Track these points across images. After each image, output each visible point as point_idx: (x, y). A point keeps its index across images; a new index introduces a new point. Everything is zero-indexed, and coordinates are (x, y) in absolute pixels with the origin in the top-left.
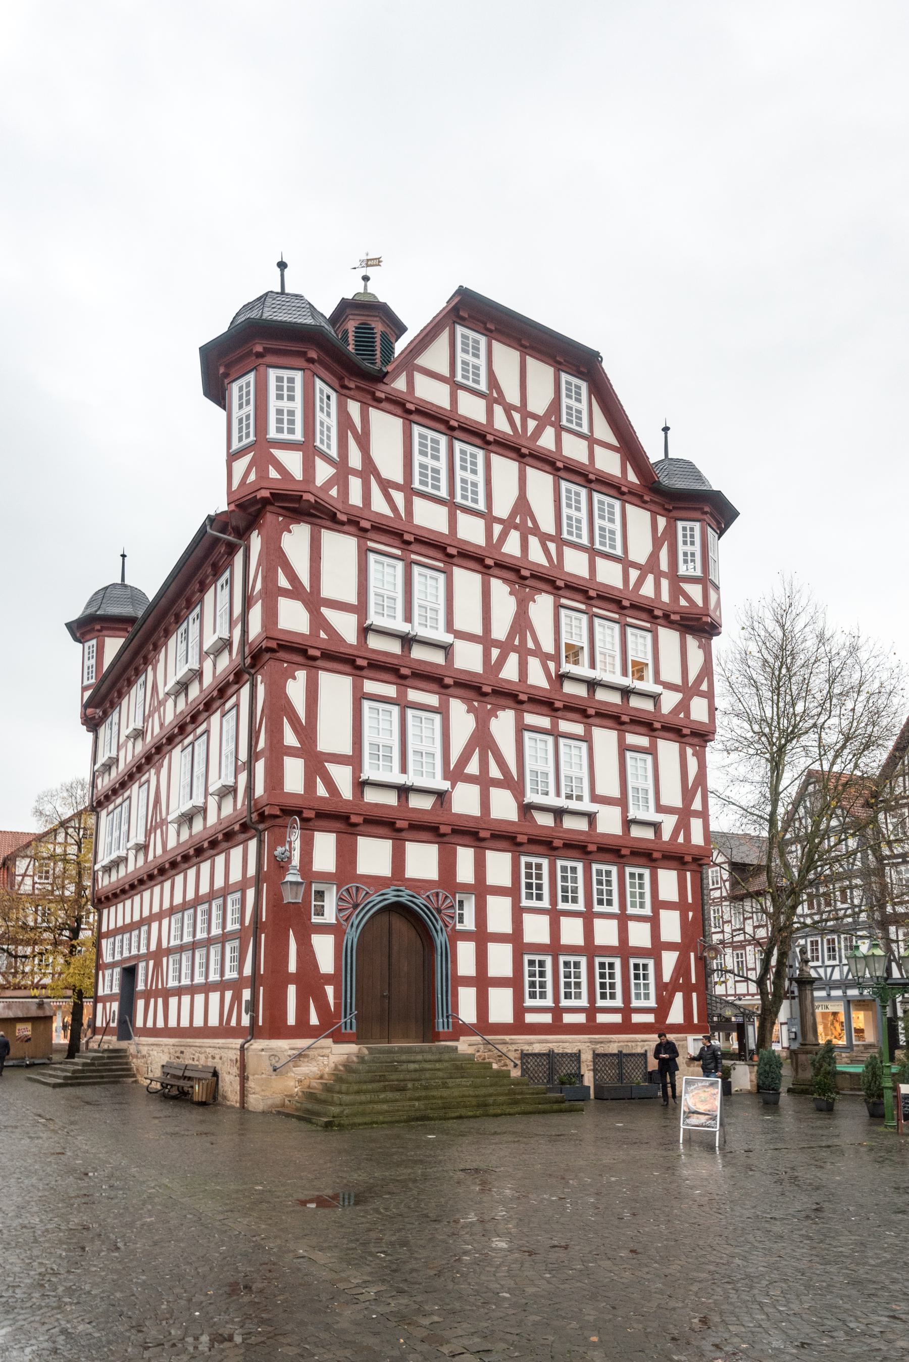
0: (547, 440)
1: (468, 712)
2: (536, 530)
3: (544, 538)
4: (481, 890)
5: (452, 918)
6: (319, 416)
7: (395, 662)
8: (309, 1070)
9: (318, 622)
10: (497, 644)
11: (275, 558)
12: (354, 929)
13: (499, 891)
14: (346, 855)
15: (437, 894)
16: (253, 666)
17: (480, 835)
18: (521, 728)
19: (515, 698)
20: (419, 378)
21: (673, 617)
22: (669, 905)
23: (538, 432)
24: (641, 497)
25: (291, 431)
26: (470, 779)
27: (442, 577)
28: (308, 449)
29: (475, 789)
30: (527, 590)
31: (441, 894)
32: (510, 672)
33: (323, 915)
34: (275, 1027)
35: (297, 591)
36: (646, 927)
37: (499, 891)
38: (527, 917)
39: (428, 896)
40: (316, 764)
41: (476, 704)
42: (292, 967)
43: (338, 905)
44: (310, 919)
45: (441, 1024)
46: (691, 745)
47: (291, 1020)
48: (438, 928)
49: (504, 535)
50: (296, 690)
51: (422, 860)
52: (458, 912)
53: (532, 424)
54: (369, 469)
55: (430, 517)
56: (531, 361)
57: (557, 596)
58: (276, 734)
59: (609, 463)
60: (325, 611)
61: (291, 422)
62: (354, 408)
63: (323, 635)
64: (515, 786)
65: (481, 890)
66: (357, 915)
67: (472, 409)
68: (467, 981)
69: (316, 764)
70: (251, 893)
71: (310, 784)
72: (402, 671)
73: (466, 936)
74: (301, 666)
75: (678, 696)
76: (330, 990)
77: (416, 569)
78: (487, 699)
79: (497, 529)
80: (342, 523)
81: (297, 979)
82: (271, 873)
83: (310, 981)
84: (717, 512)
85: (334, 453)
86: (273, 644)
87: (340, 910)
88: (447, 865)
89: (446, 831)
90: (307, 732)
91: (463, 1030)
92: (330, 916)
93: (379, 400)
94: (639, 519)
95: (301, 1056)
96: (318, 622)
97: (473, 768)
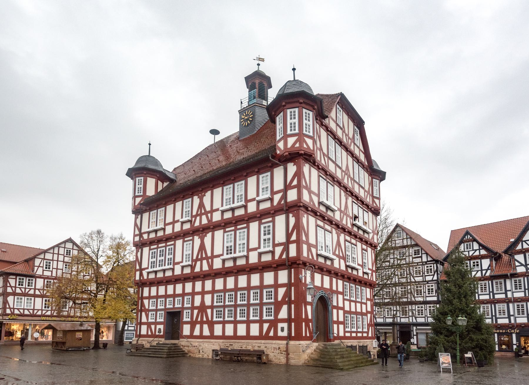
4: (337, 292)
8: (309, 351)
9: (311, 199)
11: (299, 174)
18: (346, 240)
34: (299, 337)
45: (332, 338)
47: (304, 335)
54: (321, 149)
62: (318, 126)
67: (339, 133)
72: (323, 217)
76: (310, 324)
80: (315, 166)
84: (380, 175)
86: (302, 204)
95: (308, 347)
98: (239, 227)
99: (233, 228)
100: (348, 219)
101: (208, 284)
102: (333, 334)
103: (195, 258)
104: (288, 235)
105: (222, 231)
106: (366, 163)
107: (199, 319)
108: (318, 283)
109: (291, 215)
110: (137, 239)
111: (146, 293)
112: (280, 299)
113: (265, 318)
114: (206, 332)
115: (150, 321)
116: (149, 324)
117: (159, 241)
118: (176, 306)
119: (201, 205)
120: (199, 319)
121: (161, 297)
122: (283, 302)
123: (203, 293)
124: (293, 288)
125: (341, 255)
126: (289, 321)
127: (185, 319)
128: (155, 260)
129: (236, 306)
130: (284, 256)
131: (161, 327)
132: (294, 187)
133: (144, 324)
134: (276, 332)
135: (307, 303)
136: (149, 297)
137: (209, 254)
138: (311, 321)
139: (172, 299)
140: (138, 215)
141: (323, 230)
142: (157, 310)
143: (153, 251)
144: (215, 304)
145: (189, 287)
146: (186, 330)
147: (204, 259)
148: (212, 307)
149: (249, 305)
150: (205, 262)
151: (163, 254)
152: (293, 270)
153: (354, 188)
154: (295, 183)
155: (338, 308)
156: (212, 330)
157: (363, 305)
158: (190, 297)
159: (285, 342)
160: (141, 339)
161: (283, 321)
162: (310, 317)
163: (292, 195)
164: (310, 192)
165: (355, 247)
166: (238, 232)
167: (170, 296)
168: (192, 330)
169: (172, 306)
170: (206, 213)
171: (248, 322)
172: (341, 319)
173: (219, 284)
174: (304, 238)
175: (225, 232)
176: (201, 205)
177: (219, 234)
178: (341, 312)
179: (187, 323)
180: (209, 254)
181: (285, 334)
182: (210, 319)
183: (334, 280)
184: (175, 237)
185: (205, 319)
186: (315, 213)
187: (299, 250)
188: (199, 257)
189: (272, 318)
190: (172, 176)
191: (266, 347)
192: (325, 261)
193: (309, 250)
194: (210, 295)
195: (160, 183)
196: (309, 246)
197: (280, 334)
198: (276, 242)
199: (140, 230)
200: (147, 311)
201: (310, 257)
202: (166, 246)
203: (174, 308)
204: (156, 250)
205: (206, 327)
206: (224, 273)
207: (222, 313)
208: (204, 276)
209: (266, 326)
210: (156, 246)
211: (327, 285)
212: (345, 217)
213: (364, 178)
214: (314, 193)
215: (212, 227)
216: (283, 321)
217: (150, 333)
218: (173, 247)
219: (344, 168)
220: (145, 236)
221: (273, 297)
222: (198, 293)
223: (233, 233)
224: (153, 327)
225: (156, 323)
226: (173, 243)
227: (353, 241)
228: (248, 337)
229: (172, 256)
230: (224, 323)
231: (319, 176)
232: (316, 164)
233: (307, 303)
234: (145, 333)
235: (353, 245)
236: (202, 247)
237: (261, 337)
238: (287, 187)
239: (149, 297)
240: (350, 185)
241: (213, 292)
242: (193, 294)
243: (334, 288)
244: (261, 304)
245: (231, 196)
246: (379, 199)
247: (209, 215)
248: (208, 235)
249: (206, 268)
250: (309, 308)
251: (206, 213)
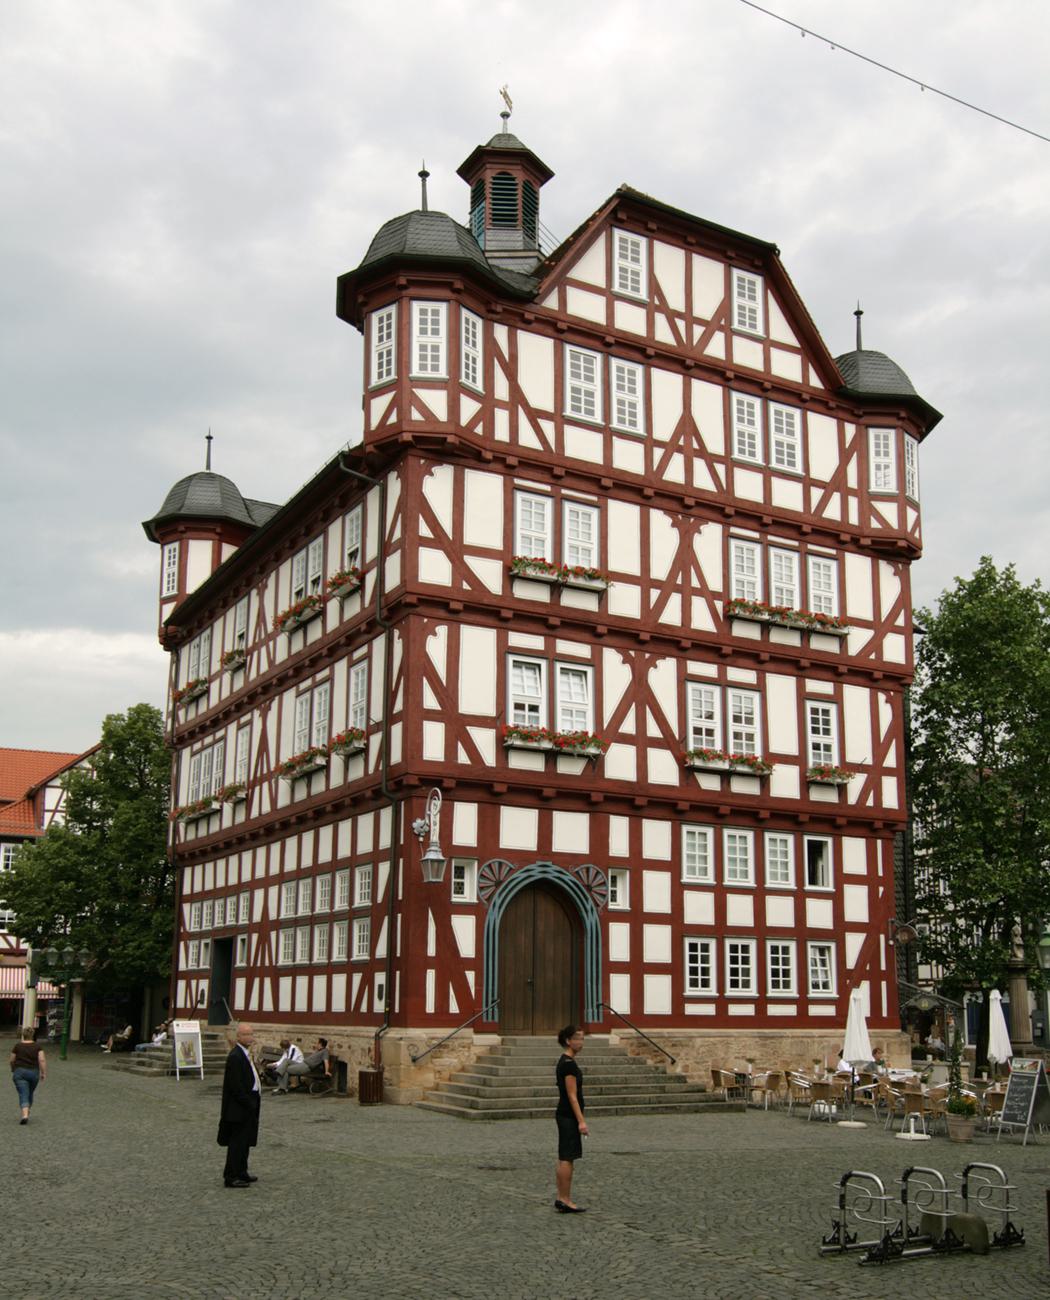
0: (716, 349)
1: (624, 662)
2: (702, 452)
4: (637, 864)
5: (604, 896)
6: (465, 348)
8: (450, 1061)
9: (461, 571)
10: (657, 584)
12: (497, 908)
13: (657, 865)
14: (489, 827)
15: (588, 869)
16: (388, 619)
17: (640, 801)
18: (684, 678)
19: (680, 644)
20: (572, 293)
22: (855, 879)
23: (706, 338)
24: (825, 404)
25: (435, 368)
26: (625, 739)
27: (595, 513)
28: (455, 388)
29: (630, 751)
30: (692, 520)
31: (591, 870)
32: (671, 616)
33: (462, 893)
35: (439, 541)
36: (828, 905)
38: (688, 895)
39: (577, 872)
40: (458, 727)
41: (632, 653)
42: (431, 951)
43: (479, 882)
44: (450, 897)
46: (884, 690)
47: (430, 1008)
48: (588, 907)
49: (665, 460)
50: (436, 647)
51: (571, 832)
52: (610, 889)
53: (698, 331)
54: (517, 397)
55: (583, 447)
56: (697, 259)
57: (726, 525)
58: (414, 696)
59: (788, 367)
60: (469, 560)
61: (435, 358)
63: (466, 586)
65: (637, 864)
66: (500, 894)
67: (631, 321)
68: (620, 967)
69: (458, 727)
70: (384, 869)
71: (450, 750)
73: (619, 916)
74: (442, 621)
75: (869, 634)
76: (471, 976)
78: (645, 647)
82: (407, 848)
83: (449, 962)
84: (918, 417)
85: (479, 387)
86: (412, 599)
87: (481, 889)
88: (599, 836)
89: (600, 799)
90: (448, 693)
91: (614, 1021)
92: (470, 895)
93: (529, 322)
94: (823, 429)
95: (441, 1046)
96: (461, 571)
97: (629, 726)
109: (396, 633)
159: (372, 1030)
164: (455, 549)
174: (430, 701)
201: (463, 758)
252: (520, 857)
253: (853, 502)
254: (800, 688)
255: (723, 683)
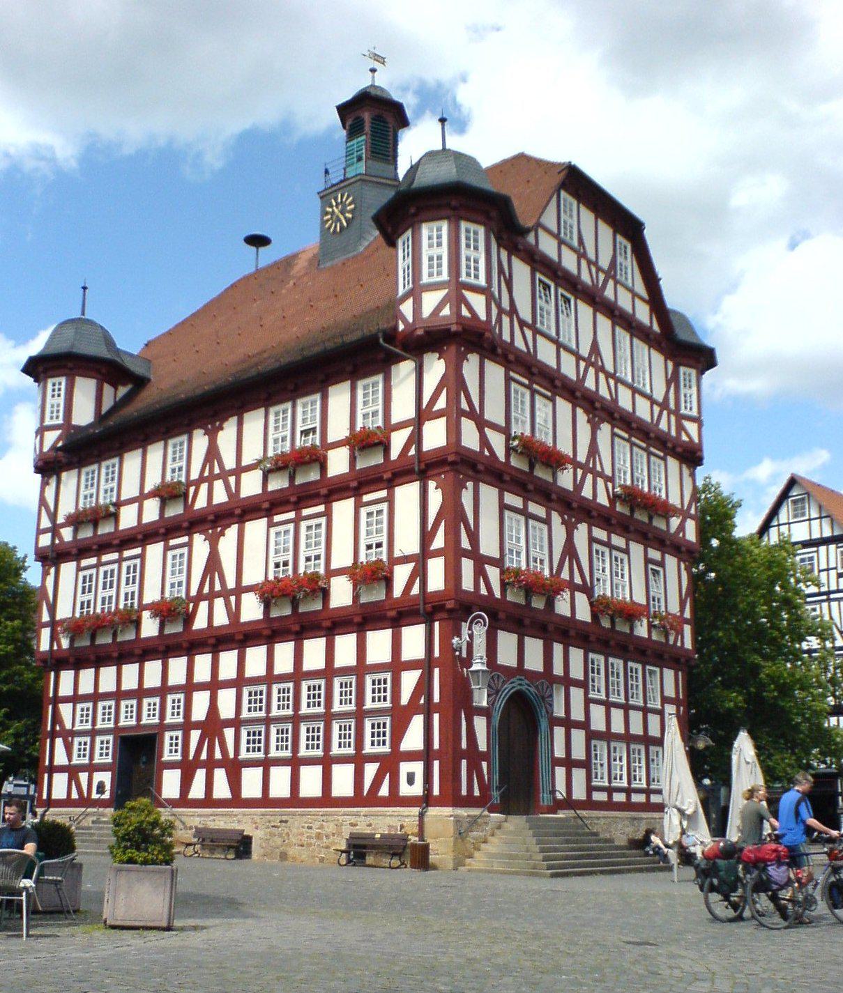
1: (562, 523)
3: (608, 375)
4: (567, 682)
7: (524, 477)
9: (484, 442)
13: (577, 683)
18: (592, 540)
21: (679, 450)
32: (587, 492)
37: (577, 683)
50: (467, 498)
60: (486, 429)
63: (487, 453)
64: (587, 590)
76: (484, 764)
77: (537, 397)
79: (582, 364)
81: (439, 755)
91: (558, 805)
94: (658, 358)
96: (484, 442)
98: (306, 512)
99: (291, 515)
100: (600, 481)
101: (228, 660)
102: (553, 792)
103: (193, 592)
104: (426, 537)
105: (263, 522)
106: (656, 328)
107: (204, 756)
108: (506, 656)
109: (432, 484)
110: (45, 540)
111: (66, 689)
112: (405, 699)
113: (368, 749)
114: (222, 789)
115: (75, 761)
116: (72, 772)
117: (101, 547)
118: (145, 721)
119: (213, 454)
120: (204, 756)
121: (107, 696)
122: (413, 708)
123: (214, 686)
124: (437, 671)
125: (578, 580)
126: (426, 755)
127: (167, 757)
128: (91, 597)
129: (296, 719)
130: (416, 590)
131: (105, 777)
132: (439, 414)
133: (61, 769)
134: (394, 785)
135: (472, 712)
136: (75, 699)
137: (231, 584)
138: (485, 756)
139: (134, 702)
140: (50, 477)
141: (522, 519)
142: (93, 733)
143: (87, 573)
144: (245, 714)
145: (177, 668)
146: (170, 784)
147: (218, 595)
148: (236, 723)
149: (328, 717)
150: (219, 603)
151: (111, 582)
152: (437, 624)
153: (615, 400)
154: (441, 403)
155: (568, 724)
156: (235, 782)
157: (650, 716)
158: (182, 696)
159: (416, 811)
160: (51, 809)
161: (411, 756)
162: (483, 747)
163: (435, 436)
164: (481, 424)
165: (625, 557)
166: (303, 525)
167: (129, 694)
168: (186, 783)
169: (133, 722)
170: (224, 475)
171: (327, 762)
172: (579, 753)
173: (256, 660)
175: (271, 525)
176: (213, 454)
177: (256, 529)
178: (578, 736)
179: (172, 765)
180: (231, 584)
181: (417, 789)
182: (232, 755)
183: (558, 649)
184: (144, 536)
185: (218, 755)
186: (499, 476)
187: (453, 573)
188: (206, 590)
189: (386, 749)
190: (138, 369)
191: (370, 825)
192: (528, 597)
193: (480, 573)
194: (233, 691)
195: (108, 389)
196: (481, 562)
197: (405, 790)
198: (397, 554)
199: (53, 516)
200: (68, 735)
201: (484, 591)
202: (120, 561)
203: (138, 726)
204: (94, 571)
205: (220, 775)
206: (267, 634)
207: (263, 737)
208: (216, 642)
209: (371, 770)
210: (93, 561)
211: (534, 662)
212: (589, 477)
213: (651, 369)
214: (494, 427)
215: (238, 511)
216: (411, 756)
217: (75, 795)
218: (138, 561)
219: (585, 351)
220: (67, 534)
221: (388, 694)
222: (202, 687)
223: (291, 527)
224: (83, 777)
225: (92, 768)
226: (138, 551)
227: (618, 541)
228: (327, 799)
229: (136, 588)
230: (266, 764)
231: (508, 380)
232: (499, 351)
233: (472, 712)
234: (64, 796)
235: (615, 553)
236: (213, 564)
237: (358, 799)
238: (423, 415)
239: (75, 699)
240: (604, 392)
241: (240, 682)
242: (190, 688)
243: (558, 670)
244: (360, 715)
245: (288, 433)
246: (697, 420)
247: (232, 480)
248: (228, 532)
249: (221, 619)
250: (480, 724)
251: (224, 475)
252: (506, 670)
253: (673, 418)
254: (646, 553)
255: (608, 544)
